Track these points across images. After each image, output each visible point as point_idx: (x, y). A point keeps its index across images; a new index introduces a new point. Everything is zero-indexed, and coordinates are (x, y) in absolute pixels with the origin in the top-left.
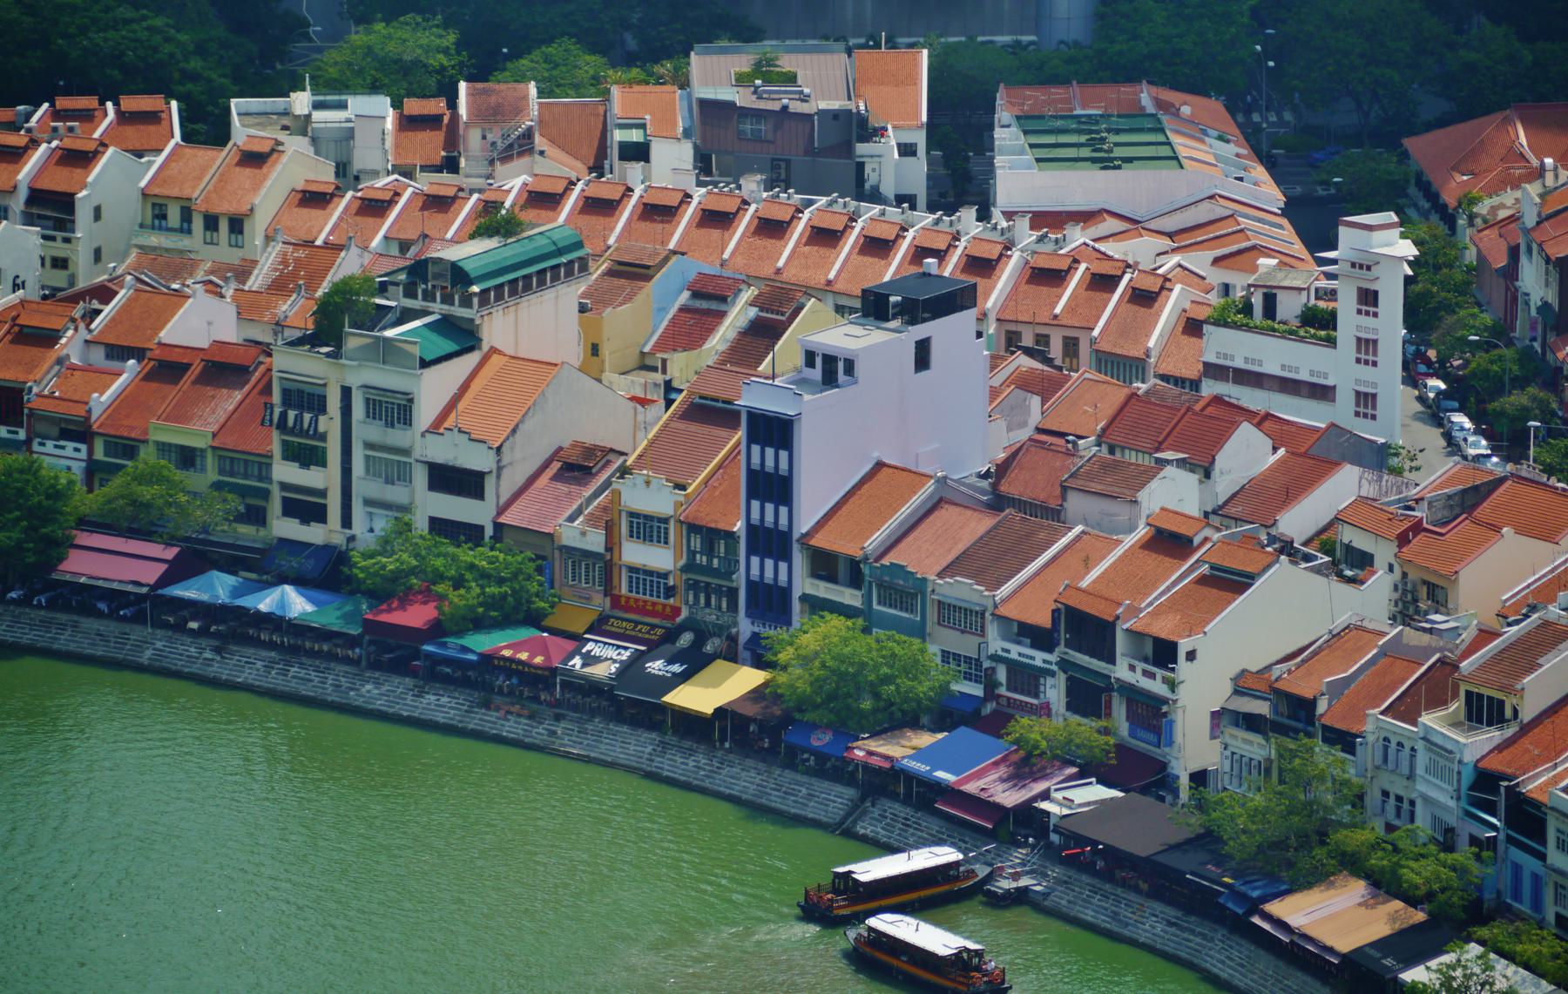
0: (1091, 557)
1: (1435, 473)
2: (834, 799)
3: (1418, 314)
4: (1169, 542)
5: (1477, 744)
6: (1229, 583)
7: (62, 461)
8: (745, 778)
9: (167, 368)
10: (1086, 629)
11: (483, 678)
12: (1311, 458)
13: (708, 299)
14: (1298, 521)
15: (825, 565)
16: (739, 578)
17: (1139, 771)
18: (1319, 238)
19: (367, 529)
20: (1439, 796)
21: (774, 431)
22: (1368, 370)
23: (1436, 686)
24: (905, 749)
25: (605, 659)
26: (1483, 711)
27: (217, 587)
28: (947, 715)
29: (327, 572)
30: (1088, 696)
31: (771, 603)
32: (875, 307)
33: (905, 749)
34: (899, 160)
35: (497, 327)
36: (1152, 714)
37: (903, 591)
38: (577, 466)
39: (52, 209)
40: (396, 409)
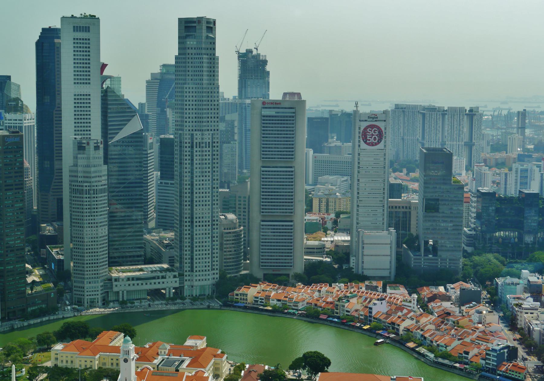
0: (394, 318)
1: (419, 313)
2: (375, 335)
3: (418, 301)
4: (399, 317)
5: (422, 332)
6: (404, 320)
7: (320, 309)
8: (368, 334)
9: (327, 303)
10: (393, 323)
11: (350, 326)
12: (410, 311)
13: (366, 299)
14: (409, 316)
15: (374, 318)
16: (368, 319)
17: (397, 334)
18: (410, 295)
19: (341, 315)
20: (419, 336)
21: (371, 308)
22: (414, 305)
23: (418, 328)
24: (380, 332)
25: (358, 325)
26: (422, 330)
27: (331, 319)
28: (383, 329)
29: (338, 318)
30: (393, 328)
31: (370, 321)
32: (378, 300)
33: (380, 332)
34: (380, 289)
35: (351, 300)
36: (398, 330)
37: (380, 320)
38: (356, 311)
39: (319, 291)
40: (344, 306)
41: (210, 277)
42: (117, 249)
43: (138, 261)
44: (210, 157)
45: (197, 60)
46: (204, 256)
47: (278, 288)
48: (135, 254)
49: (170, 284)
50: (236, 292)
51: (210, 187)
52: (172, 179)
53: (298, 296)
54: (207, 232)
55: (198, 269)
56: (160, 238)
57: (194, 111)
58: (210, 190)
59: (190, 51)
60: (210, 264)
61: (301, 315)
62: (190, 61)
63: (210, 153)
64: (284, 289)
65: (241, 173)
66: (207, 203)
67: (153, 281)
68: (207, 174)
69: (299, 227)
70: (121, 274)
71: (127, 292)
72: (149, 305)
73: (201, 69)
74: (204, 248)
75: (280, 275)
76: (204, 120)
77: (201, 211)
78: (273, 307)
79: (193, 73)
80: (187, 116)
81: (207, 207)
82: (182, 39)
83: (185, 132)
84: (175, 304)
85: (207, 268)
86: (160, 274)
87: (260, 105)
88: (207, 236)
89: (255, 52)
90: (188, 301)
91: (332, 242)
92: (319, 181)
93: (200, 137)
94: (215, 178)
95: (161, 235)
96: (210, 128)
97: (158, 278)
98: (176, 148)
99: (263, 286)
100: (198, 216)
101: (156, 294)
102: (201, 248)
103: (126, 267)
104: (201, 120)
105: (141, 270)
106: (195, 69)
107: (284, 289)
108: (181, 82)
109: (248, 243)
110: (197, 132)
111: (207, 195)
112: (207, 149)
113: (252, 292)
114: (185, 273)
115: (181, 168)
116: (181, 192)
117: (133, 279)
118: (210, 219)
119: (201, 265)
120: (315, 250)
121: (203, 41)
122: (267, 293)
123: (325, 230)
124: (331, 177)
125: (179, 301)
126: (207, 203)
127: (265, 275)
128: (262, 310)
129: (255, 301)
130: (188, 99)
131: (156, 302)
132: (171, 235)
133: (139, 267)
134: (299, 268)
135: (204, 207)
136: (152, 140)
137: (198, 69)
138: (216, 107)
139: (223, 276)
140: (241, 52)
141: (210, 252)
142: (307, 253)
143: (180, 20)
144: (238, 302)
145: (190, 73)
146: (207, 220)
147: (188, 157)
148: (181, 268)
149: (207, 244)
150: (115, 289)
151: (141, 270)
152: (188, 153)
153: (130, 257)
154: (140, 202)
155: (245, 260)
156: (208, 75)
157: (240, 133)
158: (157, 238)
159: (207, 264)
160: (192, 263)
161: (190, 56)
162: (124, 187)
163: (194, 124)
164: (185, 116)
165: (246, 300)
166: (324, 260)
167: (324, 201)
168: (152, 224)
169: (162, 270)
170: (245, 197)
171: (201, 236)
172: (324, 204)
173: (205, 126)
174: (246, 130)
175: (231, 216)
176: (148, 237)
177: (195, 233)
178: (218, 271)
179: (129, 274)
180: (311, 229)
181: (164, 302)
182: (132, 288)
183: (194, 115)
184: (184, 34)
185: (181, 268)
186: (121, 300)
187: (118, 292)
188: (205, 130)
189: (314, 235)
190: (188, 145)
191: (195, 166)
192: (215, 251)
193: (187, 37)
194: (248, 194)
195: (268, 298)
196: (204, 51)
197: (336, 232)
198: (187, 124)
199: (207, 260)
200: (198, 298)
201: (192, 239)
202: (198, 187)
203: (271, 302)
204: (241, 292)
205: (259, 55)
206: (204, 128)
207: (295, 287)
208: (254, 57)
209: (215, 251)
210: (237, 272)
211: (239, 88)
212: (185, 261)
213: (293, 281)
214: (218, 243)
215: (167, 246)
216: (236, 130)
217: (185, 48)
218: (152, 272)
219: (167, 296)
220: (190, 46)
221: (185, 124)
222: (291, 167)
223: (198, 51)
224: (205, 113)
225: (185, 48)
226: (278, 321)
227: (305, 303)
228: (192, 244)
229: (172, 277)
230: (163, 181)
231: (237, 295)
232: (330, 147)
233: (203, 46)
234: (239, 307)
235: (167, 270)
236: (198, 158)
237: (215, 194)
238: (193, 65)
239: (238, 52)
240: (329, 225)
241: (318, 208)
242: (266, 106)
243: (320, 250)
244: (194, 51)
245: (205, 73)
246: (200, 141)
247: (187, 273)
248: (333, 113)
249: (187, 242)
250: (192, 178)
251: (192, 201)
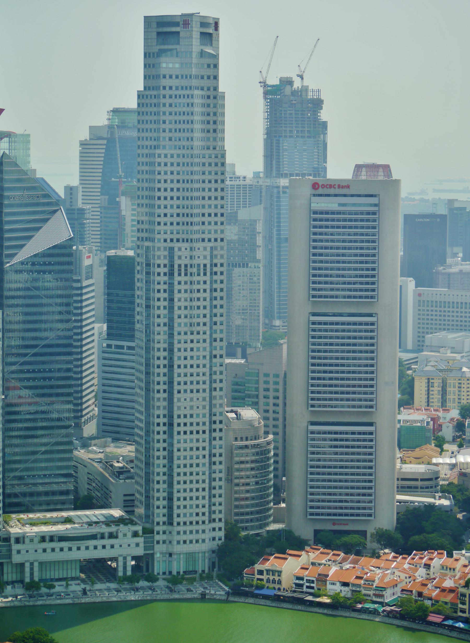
7: (428, 603)
9: (443, 590)
27: (450, 622)
39: (427, 566)
41: (207, 536)
42: (21, 478)
43: (63, 503)
44: (207, 295)
45: (182, 101)
46: (194, 494)
47: (344, 560)
48: (55, 488)
49: (125, 548)
50: (258, 567)
51: (207, 354)
52: (132, 338)
53: (385, 576)
54: (201, 445)
55: (181, 520)
56: (106, 456)
57: (175, 202)
58: (207, 362)
59: (166, 82)
60: (206, 510)
61: (389, 614)
62: (167, 101)
63: (207, 287)
64: (355, 562)
65: (269, 326)
66: (201, 387)
67: (92, 543)
68: (201, 328)
69: (386, 437)
70: (27, 529)
71: (41, 564)
72: (84, 592)
73: (190, 118)
74: (194, 478)
75: (348, 533)
76: (196, 219)
77: (191, 405)
78: (335, 597)
79: (173, 126)
80: (162, 211)
81: (201, 395)
83: (157, 245)
84: (137, 589)
85: (200, 518)
86: (106, 530)
87: (307, 190)
88: (201, 453)
89: (297, 84)
90: (161, 583)
91: (453, 466)
92: (427, 343)
93: (187, 253)
94: (217, 336)
95: (108, 450)
96: (206, 236)
97: (103, 537)
98: (138, 276)
99: (312, 555)
100: (182, 413)
101: (98, 569)
102: (188, 478)
103: (39, 515)
104: (189, 219)
105: (68, 520)
106: (177, 118)
107: (355, 562)
108: (149, 143)
109: (283, 469)
110: (180, 244)
111: (201, 370)
112: (202, 278)
113: (290, 568)
114: (157, 528)
115: (148, 316)
116: (148, 365)
117: (52, 539)
118: (207, 420)
119: (188, 511)
120: (419, 483)
121: (194, 61)
122: (320, 570)
123: (440, 443)
124: (451, 336)
125: (143, 583)
126: (201, 387)
127: (316, 532)
128: (311, 603)
129: (297, 585)
130: (162, 177)
131: (99, 586)
132: (126, 450)
133: (65, 514)
134: (386, 519)
135: (195, 395)
136: (91, 260)
137: (182, 118)
138: (219, 194)
139: (231, 534)
141: (206, 485)
142: (402, 489)
143: (149, 21)
144: (262, 587)
145: (167, 126)
146: (201, 420)
147: (162, 295)
148: (147, 516)
149: (200, 469)
150: (16, 559)
151: (68, 520)
152: (162, 287)
153: (46, 494)
154: (66, 386)
155: (277, 502)
156: (203, 131)
158: (101, 456)
159: (201, 510)
160: (170, 508)
161: (167, 92)
162: (35, 355)
163: (175, 227)
164: (157, 211)
165: (280, 582)
166: (438, 502)
167: (437, 383)
168: (90, 429)
169: (110, 521)
170: (277, 376)
171: (188, 453)
172: (436, 389)
173: (197, 232)
174: (279, 239)
175: (249, 414)
176: (81, 453)
177: (176, 446)
178: (222, 525)
179: (44, 529)
180: (410, 439)
181: (113, 585)
182: (49, 557)
183: (175, 211)
184: (156, 49)
185: (148, 517)
186: (27, 580)
187: (22, 565)
188: (197, 240)
189: (417, 452)
190: (162, 270)
191: (177, 312)
192: (216, 484)
193: (161, 53)
194: (284, 368)
195: (322, 579)
196: (195, 83)
197: (461, 446)
198: (162, 228)
199: (200, 502)
200: (183, 578)
201: (170, 459)
202: (183, 354)
203: (329, 586)
204: (267, 566)
205: (305, 89)
206: (195, 236)
207: (378, 557)
208: (294, 93)
209: (216, 484)
210: (261, 527)
211: (265, 156)
212: (157, 503)
213: (375, 545)
214: (222, 467)
215: (120, 473)
216: (260, 241)
217: (158, 77)
218: (90, 524)
219: (120, 574)
220: (167, 73)
221: (157, 228)
222: (370, 315)
223: (184, 82)
224: (198, 207)
225: (158, 77)
226: (344, 624)
227: (398, 589)
228: (171, 468)
229: (129, 535)
230: (113, 343)
231: (261, 572)
232: (449, 274)
233: (194, 71)
234: (266, 597)
235: (120, 521)
236: (183, 295)
237: (217, 369)
238: (173, 109)
239: (264, 84)
240: (448, 432)
241: (424, 397)
242: (320, 191)
243: (429, 483)
244: (174, 82)
246: (188, 262)
247: (161, 528)
248: (456, 205)
249: (159, 466)
250: (171, 336)
251: (171, 383)
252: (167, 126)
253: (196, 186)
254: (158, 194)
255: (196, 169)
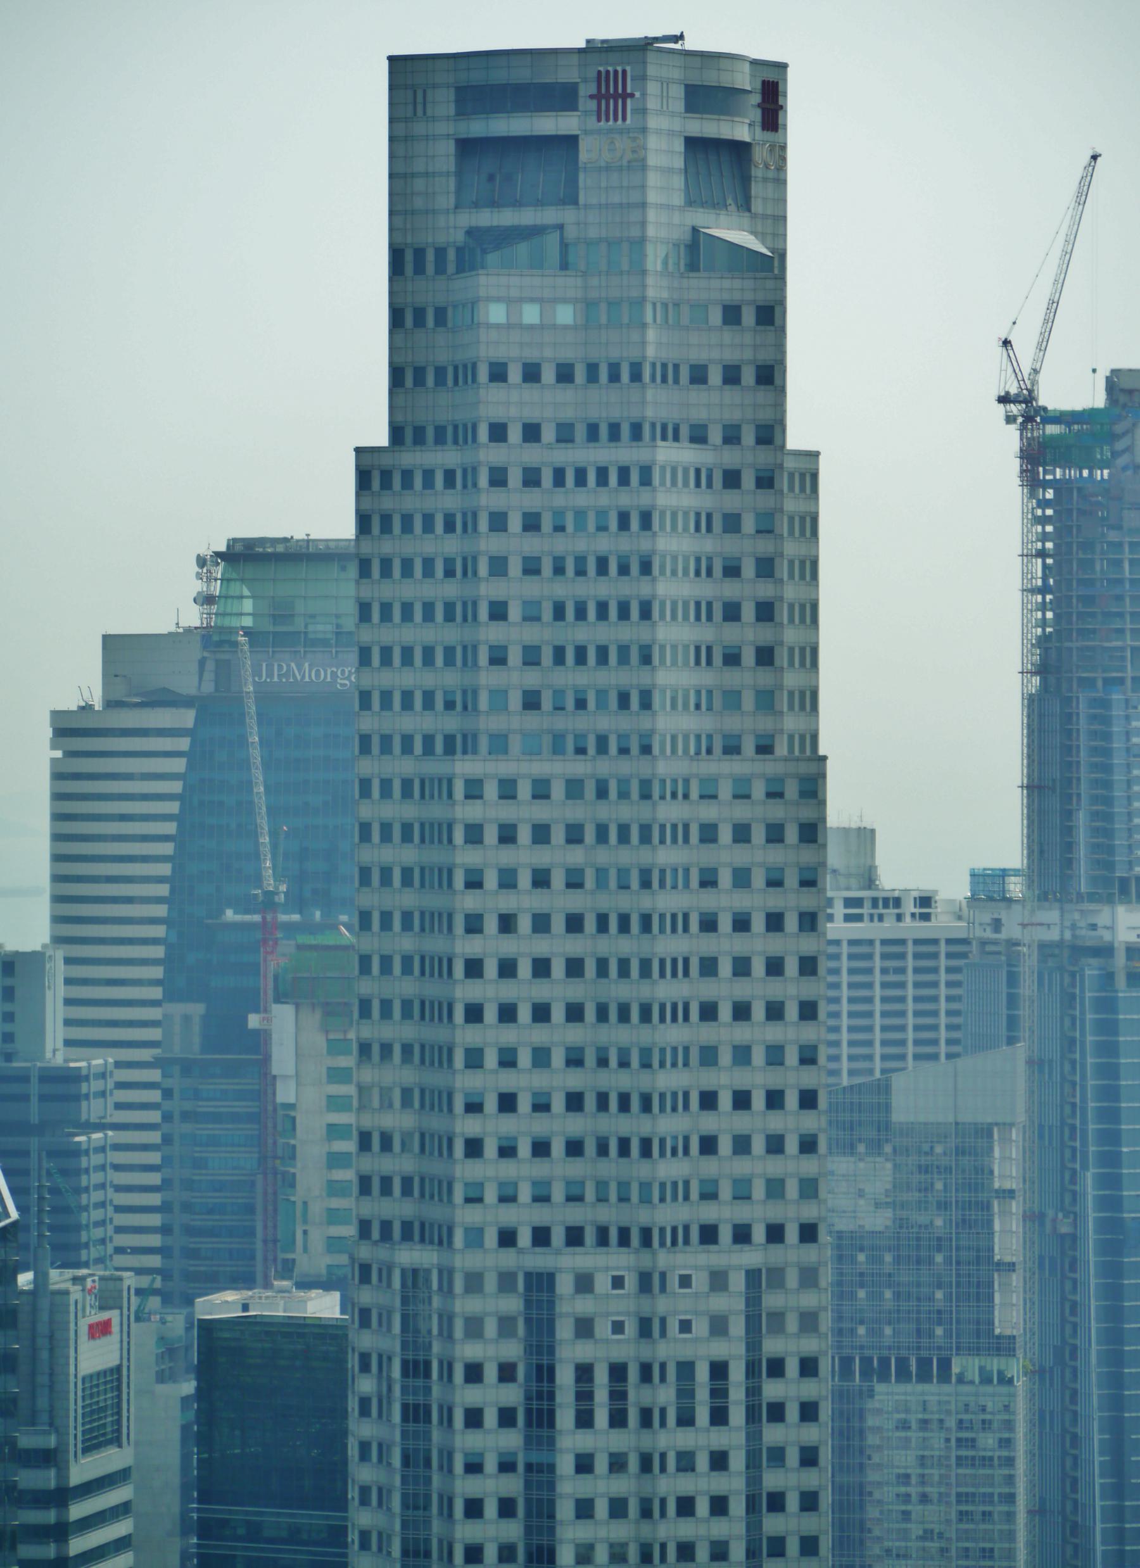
45: (590, 498)
57: (560, 1035)
62: (516, 501)
63: (733, 1484)
73: (633, 588)
76: (668, 1125)
79: (544, 634)
80: (490, 1081)
82: (421, 272)
83: (464, 1261)
93: (626, 1304)
96: (724, 1213)
98: (361, 1429)
104: (634, 1125)
106: (568, 589)
108: (417, 723)
112: (702, 1438)
121: (656, 289)
130: (491, 902)
138: (791, 989)
140: (1051, 398)
145: (514, 634)
152: (491, 1486)
156: (703, 655)
157: (1057, 1261)
161: (515, 455)
163: (560, 1168)
164: (465, 1082)
183: (560, 1080)
188: (678, 1237)
190: (492, 1395)
196: (658, 403)
198: (489, 1170)
206: (667, 1215)
216: (1009, 1236)
217: (465, 373)
220: (513, 353)
221: (465, 1170)
223: (604, 403)
224: (679, 1057)
233: (655, 344)
239: (1022, 405)
244: (549, 403)
245: (673, 633)
246: (628, 1349)
252: (514, 634)
253: (668, 946)
254: (465, 991)
255: (666, 856)
